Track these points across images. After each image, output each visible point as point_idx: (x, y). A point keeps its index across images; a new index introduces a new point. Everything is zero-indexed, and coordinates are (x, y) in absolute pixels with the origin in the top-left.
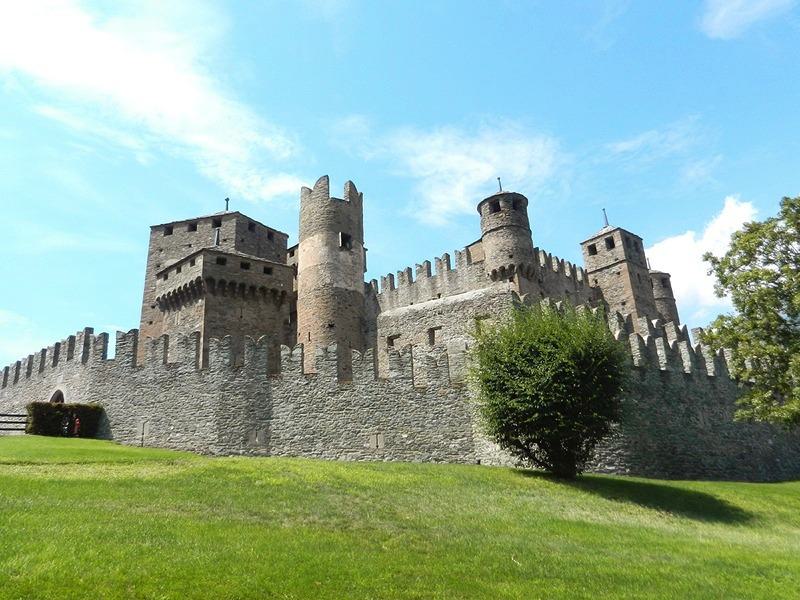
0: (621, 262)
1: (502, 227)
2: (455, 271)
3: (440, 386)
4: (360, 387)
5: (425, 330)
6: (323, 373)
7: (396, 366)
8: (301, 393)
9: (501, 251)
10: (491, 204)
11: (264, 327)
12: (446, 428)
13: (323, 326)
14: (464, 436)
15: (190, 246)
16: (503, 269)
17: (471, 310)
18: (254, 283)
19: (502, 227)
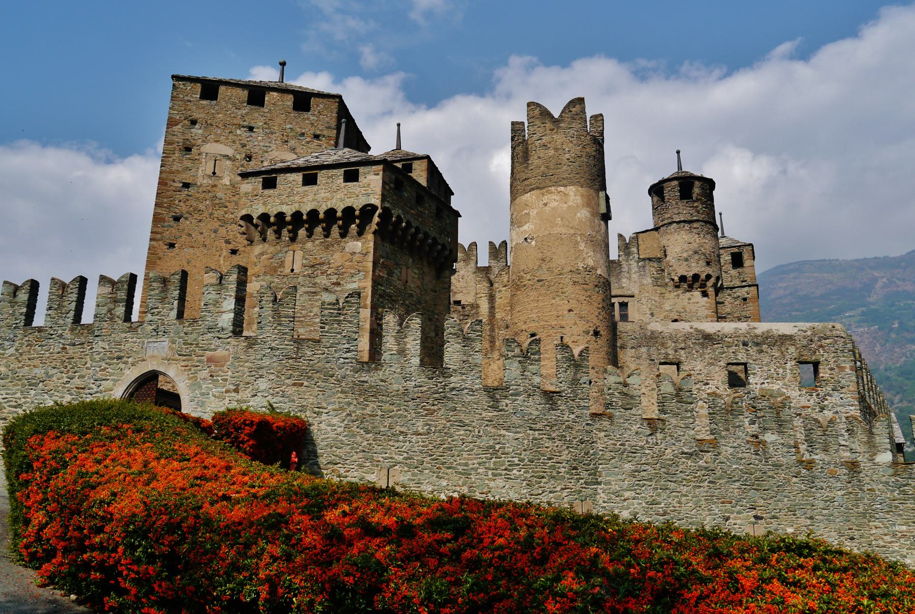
0: (749, 286)
1: (697, 221)
2: (618, 263)
3: (829, 463)
4: (727, 450)
5: (722, 363)
6: (674, 421)
7: (774, 425)
8: (642, 447)
9: (696, 252)
10: (680, 185)
11: (426, 302)
12: (839, 523)
13: (587, 333)
14: (861, 537)
15: (251, 129)
16: (696, 277)
17: (792, 349)
18: (427, 230)
19: (697, 221)
